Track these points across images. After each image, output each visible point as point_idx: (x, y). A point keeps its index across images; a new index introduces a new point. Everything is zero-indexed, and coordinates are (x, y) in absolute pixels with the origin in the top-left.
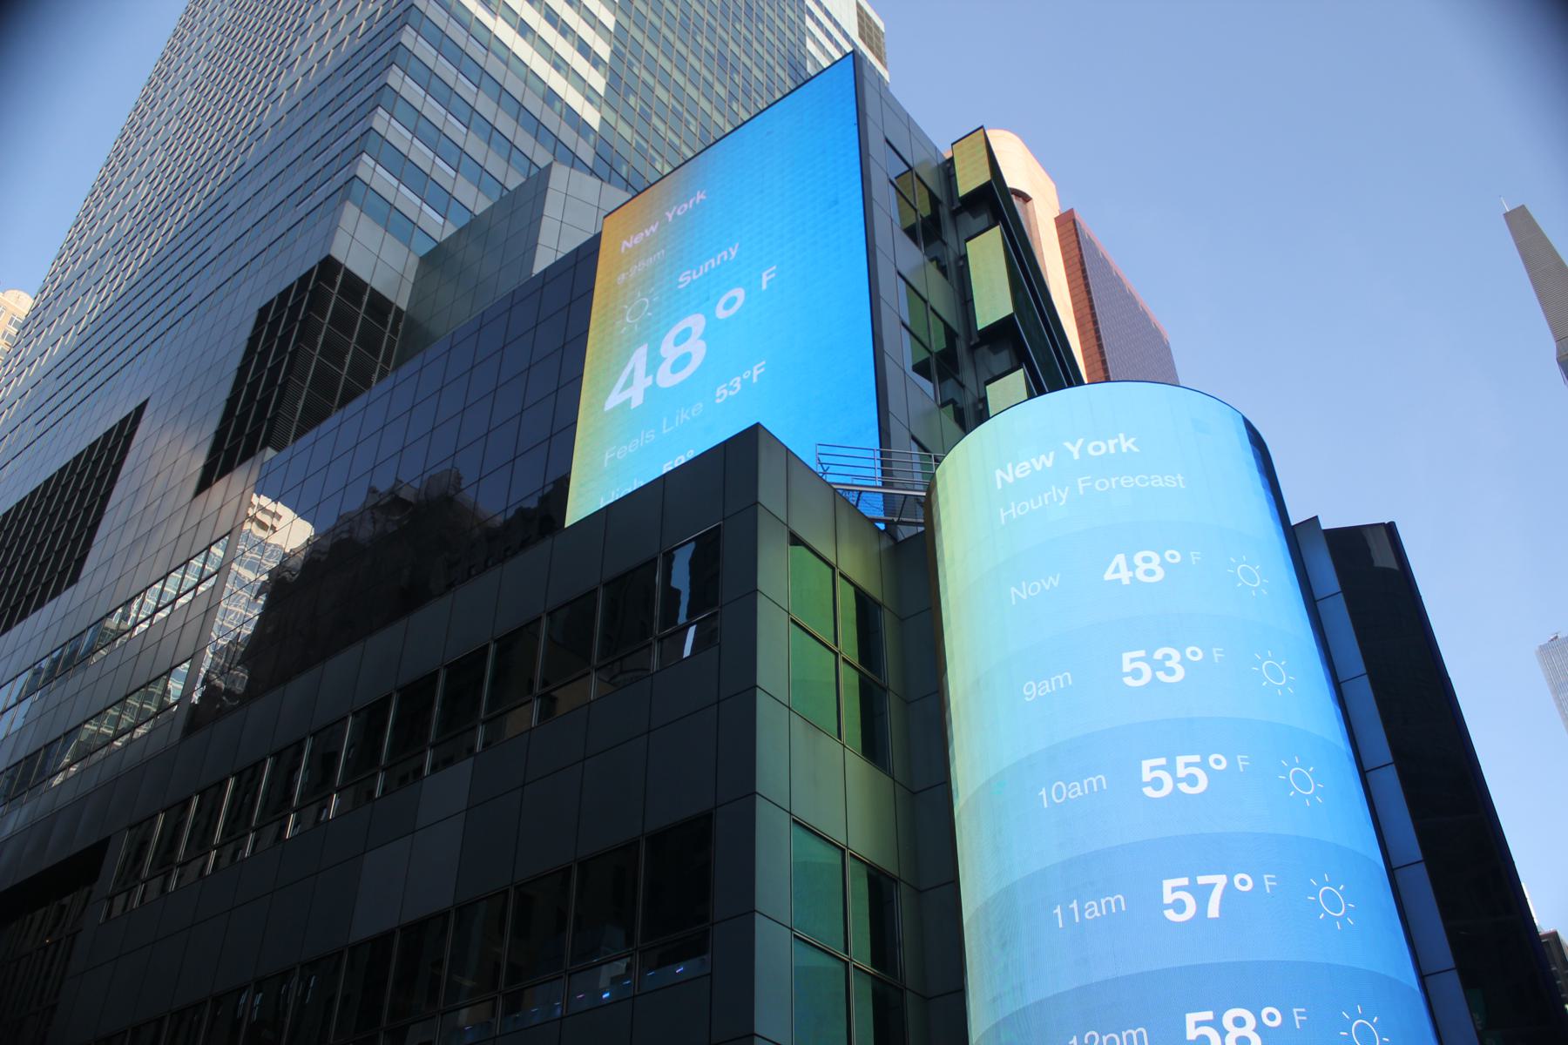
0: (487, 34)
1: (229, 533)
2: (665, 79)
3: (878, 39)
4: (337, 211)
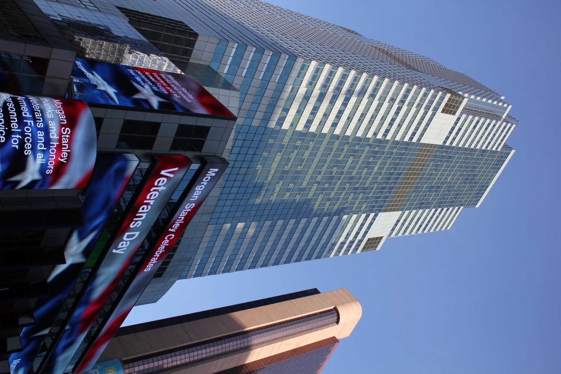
2: (313, 155)
3: (372, 247)
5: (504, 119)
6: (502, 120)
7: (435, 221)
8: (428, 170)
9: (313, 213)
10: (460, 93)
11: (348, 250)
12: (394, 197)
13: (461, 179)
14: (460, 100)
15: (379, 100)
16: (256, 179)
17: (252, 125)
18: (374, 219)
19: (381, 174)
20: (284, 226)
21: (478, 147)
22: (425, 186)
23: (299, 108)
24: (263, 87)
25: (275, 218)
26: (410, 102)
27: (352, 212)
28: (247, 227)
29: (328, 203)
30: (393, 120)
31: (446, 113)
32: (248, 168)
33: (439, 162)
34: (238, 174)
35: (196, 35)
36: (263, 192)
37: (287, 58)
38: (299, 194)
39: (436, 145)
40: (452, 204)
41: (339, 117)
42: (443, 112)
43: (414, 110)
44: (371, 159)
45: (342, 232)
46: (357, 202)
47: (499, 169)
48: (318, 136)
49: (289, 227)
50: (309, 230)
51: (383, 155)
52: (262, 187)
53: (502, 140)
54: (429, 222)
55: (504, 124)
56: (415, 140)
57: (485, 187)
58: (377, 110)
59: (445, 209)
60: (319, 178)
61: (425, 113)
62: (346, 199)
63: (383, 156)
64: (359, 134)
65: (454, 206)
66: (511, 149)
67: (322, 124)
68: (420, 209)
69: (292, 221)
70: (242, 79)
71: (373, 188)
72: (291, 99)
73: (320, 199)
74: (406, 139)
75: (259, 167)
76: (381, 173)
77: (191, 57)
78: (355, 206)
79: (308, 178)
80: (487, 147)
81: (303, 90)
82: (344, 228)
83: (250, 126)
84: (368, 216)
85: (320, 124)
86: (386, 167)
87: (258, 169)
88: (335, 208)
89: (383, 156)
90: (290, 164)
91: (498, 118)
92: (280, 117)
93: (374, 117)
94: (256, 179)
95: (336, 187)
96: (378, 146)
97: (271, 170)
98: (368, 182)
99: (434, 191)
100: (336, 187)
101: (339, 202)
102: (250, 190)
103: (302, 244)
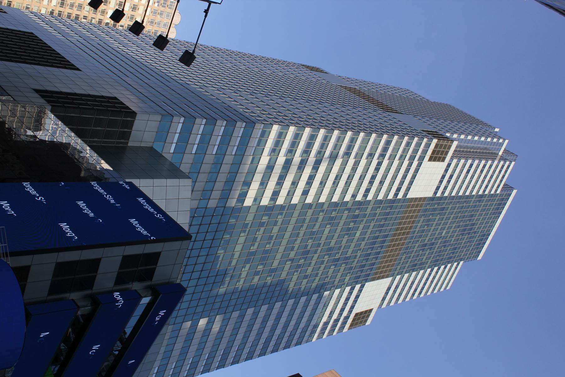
0: (260, 154)
1: (15, 100)
2: (283, 230)
3: (361, 323)
4: (157, 113)
5: (501, 157)
6: (498, 157)
7: (432, 282)
8: (418, 227)
9: (288, 295)
10: (448, 135)
11: (333, 330)
12: (381, 263)
13: (457, 231)
14: (449, 144)
15: (355, 158)
16: (218, 267)
17: (208, 206)
18: (360, 291)
19: (365, 239)
20: (256, 314)
21: (474, 193)
22: (417, 245)
23: (262, 180)
24: (218, 163)
25: (244, 307)
26: (391, 155)
27: (334, 286)
28: (210, 323)
29: (305, 281)
30: (373, 177)
31: (434, 160)
32: (207, 255)
33: (431, 216)
34: (195, 264)
35: (133, 114)
36: (228, 279)
37: (243, 126)
38: (271, 276)
39: (425, 198)
40: (450, 260)
41: (310, 182)
42: (430, 160)
43: (396, 162)
44: (352, 225)
45: (324, 310)
46: (339, 275)
47: (500, 213)
48: (288, 208)
49: (261, 315)
50: (285, 314)
51: (365, 218)
52: (225, 274)
53: (501, 181)
54: (425, 284)
55: (502, 163)
56: (400, 196)
57: (486, 235)
58: (354, 169)
59: (443, 267)
60: (292, 255)
61: (410, 165)
62: (325, 273)
63: (365, 219)
64: (335, 199)
65: (452, 263)
66: (512, 189)
67: (291, 194)
68: (413, 272)
69: (264, 308)
70: (192, 156)
71: (356, 256)
72: (252, 172)
73: (295, 278)
74: (391, 196)
75: (221, 252)
76: (364, 238)
77: (130, 140)
78: (337, 280)
79: (279, 256)
80: (484, 191)
81: (264, 160)
82: (326, 306)
83: (206, 208)
84: (353, 289)
85: (288, 195)
86: (369, 231)
87: (220, 255)
88: (314, 285)
89: (365, 219)
90: (257, 244)
91: (492, 156)
92: (241, 192)
93: (350, 178)
94: (218, 267)
95: (313, 262)
96: (359, 209)
97: (235, 254)
98: (350, 251)
99: (428, 248)
100: (313, 262)
101: (317, 279)
102: (211, 280)
103: (278, 332)
